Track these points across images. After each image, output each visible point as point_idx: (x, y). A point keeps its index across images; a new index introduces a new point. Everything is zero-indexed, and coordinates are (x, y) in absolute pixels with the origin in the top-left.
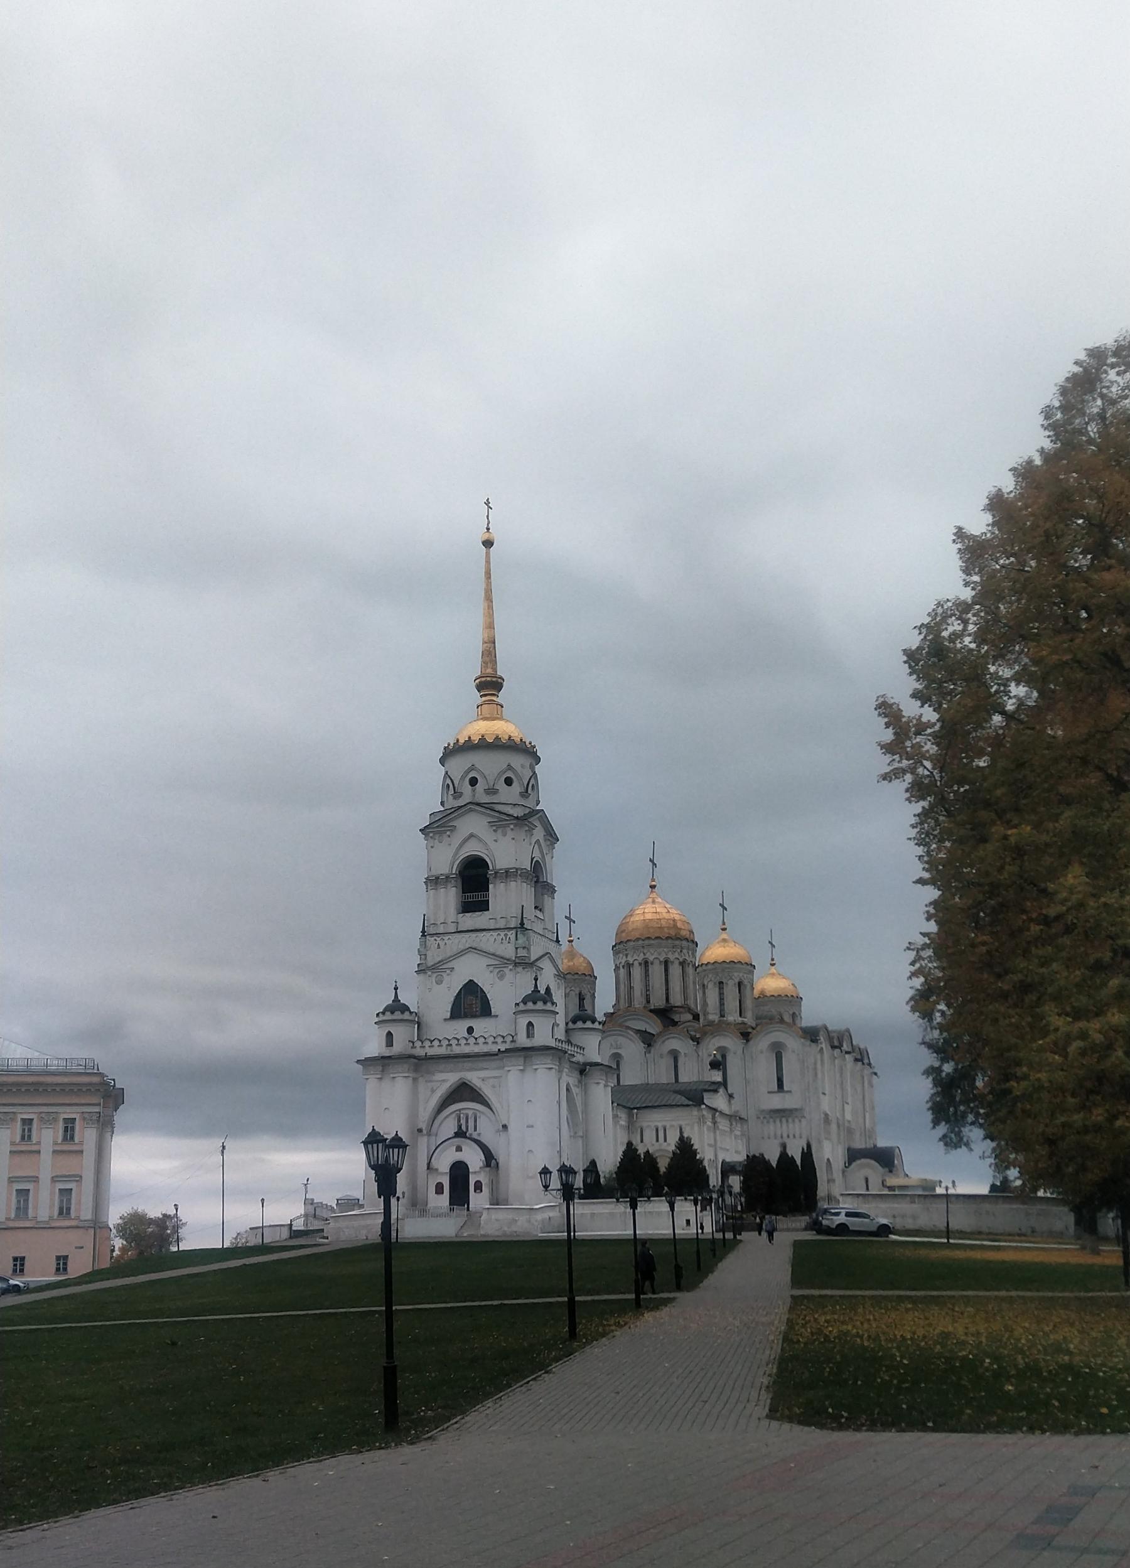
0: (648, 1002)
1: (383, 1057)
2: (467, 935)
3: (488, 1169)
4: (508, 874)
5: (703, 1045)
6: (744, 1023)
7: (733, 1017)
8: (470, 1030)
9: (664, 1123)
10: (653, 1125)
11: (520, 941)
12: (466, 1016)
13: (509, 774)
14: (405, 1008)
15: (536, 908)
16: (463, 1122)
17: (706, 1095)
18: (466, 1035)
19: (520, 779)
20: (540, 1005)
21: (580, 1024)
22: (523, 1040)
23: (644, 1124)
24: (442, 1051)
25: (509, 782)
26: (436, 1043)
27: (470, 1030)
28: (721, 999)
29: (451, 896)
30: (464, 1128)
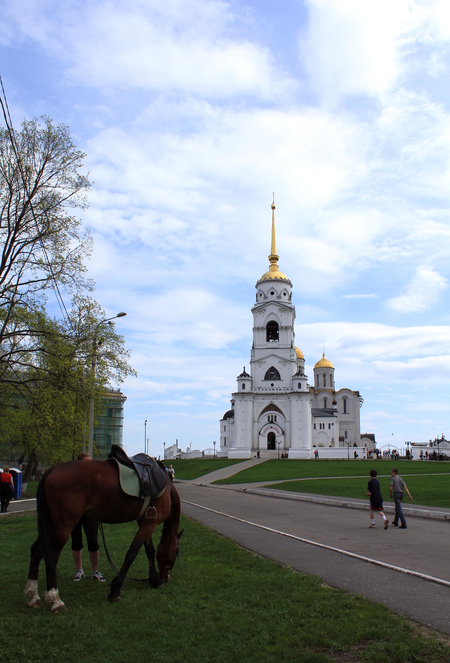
1: (242, 393)
2: (271, 350)
4: (287, 328)
5: (319, 395)
8: (272, 385)
9: (323, 422)
10: (319, 423)
11: (291, 353)
12: (270, 379)
13: (285, 292)
14: (249, 376)
16: (270, 418)
18: (270, 386)
19: (288, 294)
22: (296, 389)
23: (316, 423)
24: (264, 392)
25: (285, 294)
26: (261, 389)
27: (272, 385)
28: (325, 381)
29: (264, 334)
30: (274, 421)
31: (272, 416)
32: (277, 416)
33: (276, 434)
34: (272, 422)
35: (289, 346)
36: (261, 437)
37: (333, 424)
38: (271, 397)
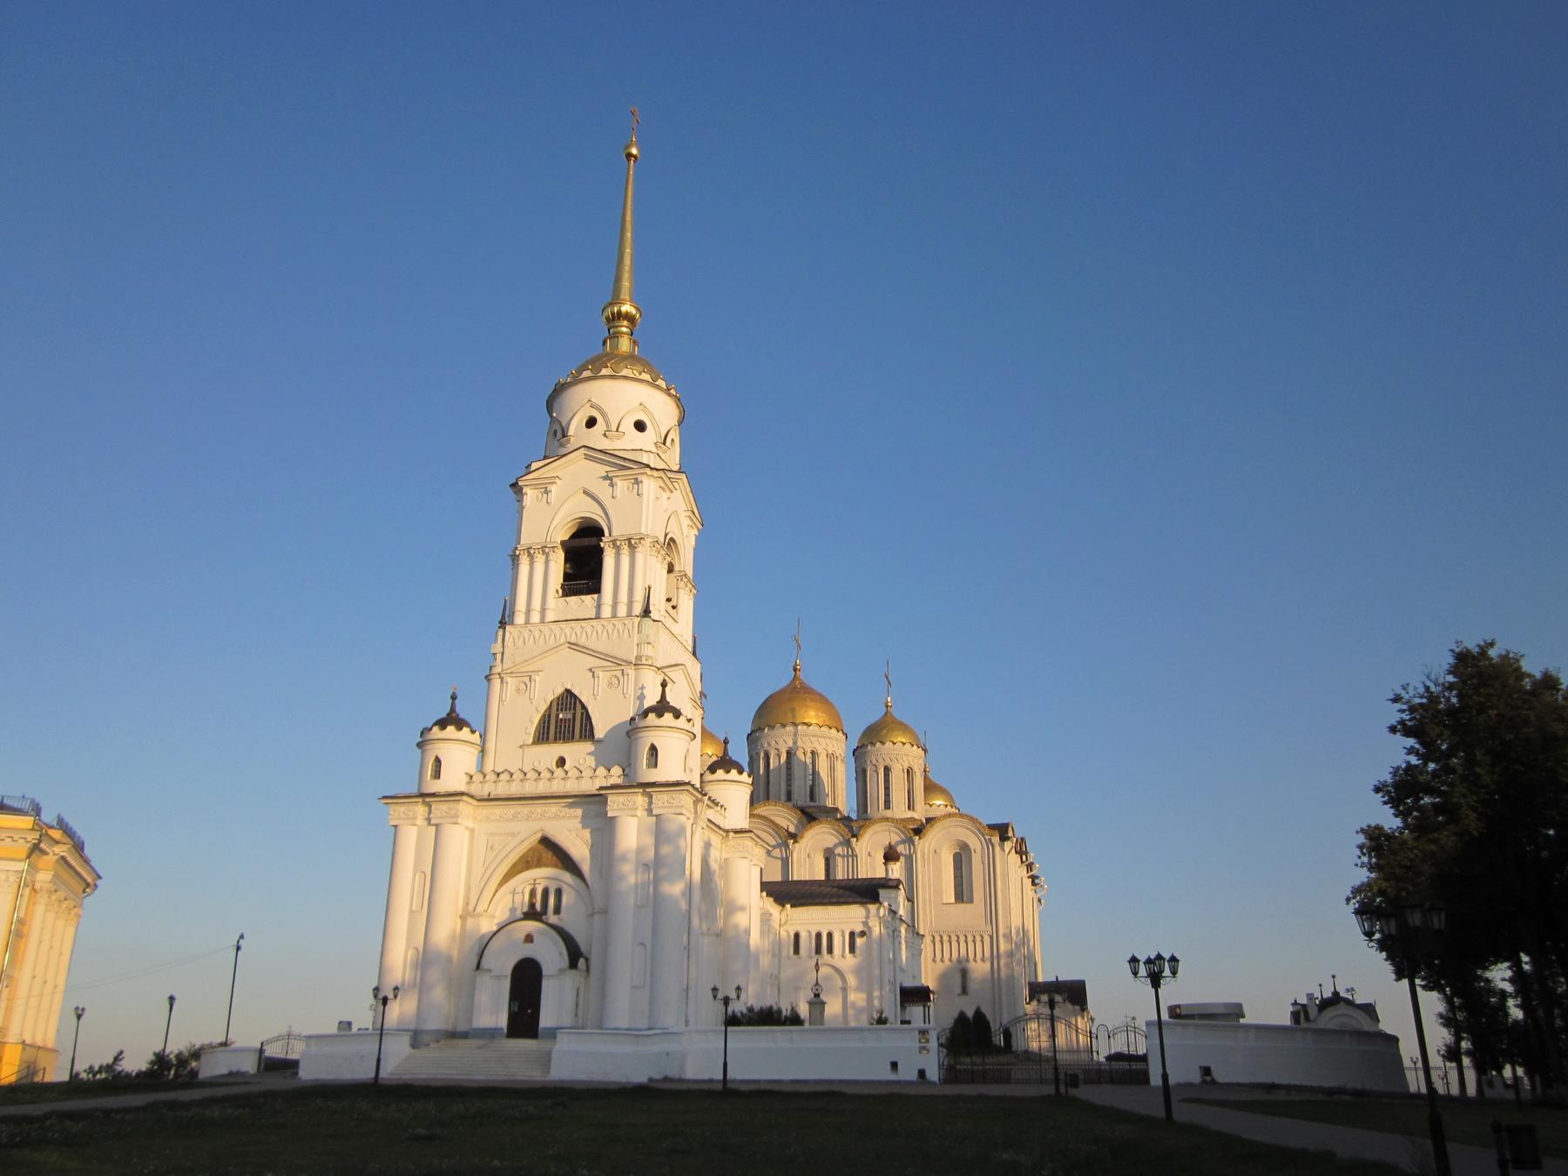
0: (789, 797)
3: (574, 972)
6: (912, 820)
7: (899, 810)
8: (561, 762)
12: (555, 740)
15: (669, 600)
17: (882, 893)
19: (656, 426)
20: (668, 716)
21: (720, 773)
24: (515, 789)
25: (640, 426)
26: (505, 777)
27: (561, 762)
30: (538, 907)
31: (546, 892)
32: (565, 889)
33: (547, 969)
34: (532, 914)
35: (638, 608)
36: (484, 981)
37: (863, 934)
38: (539, 808)
